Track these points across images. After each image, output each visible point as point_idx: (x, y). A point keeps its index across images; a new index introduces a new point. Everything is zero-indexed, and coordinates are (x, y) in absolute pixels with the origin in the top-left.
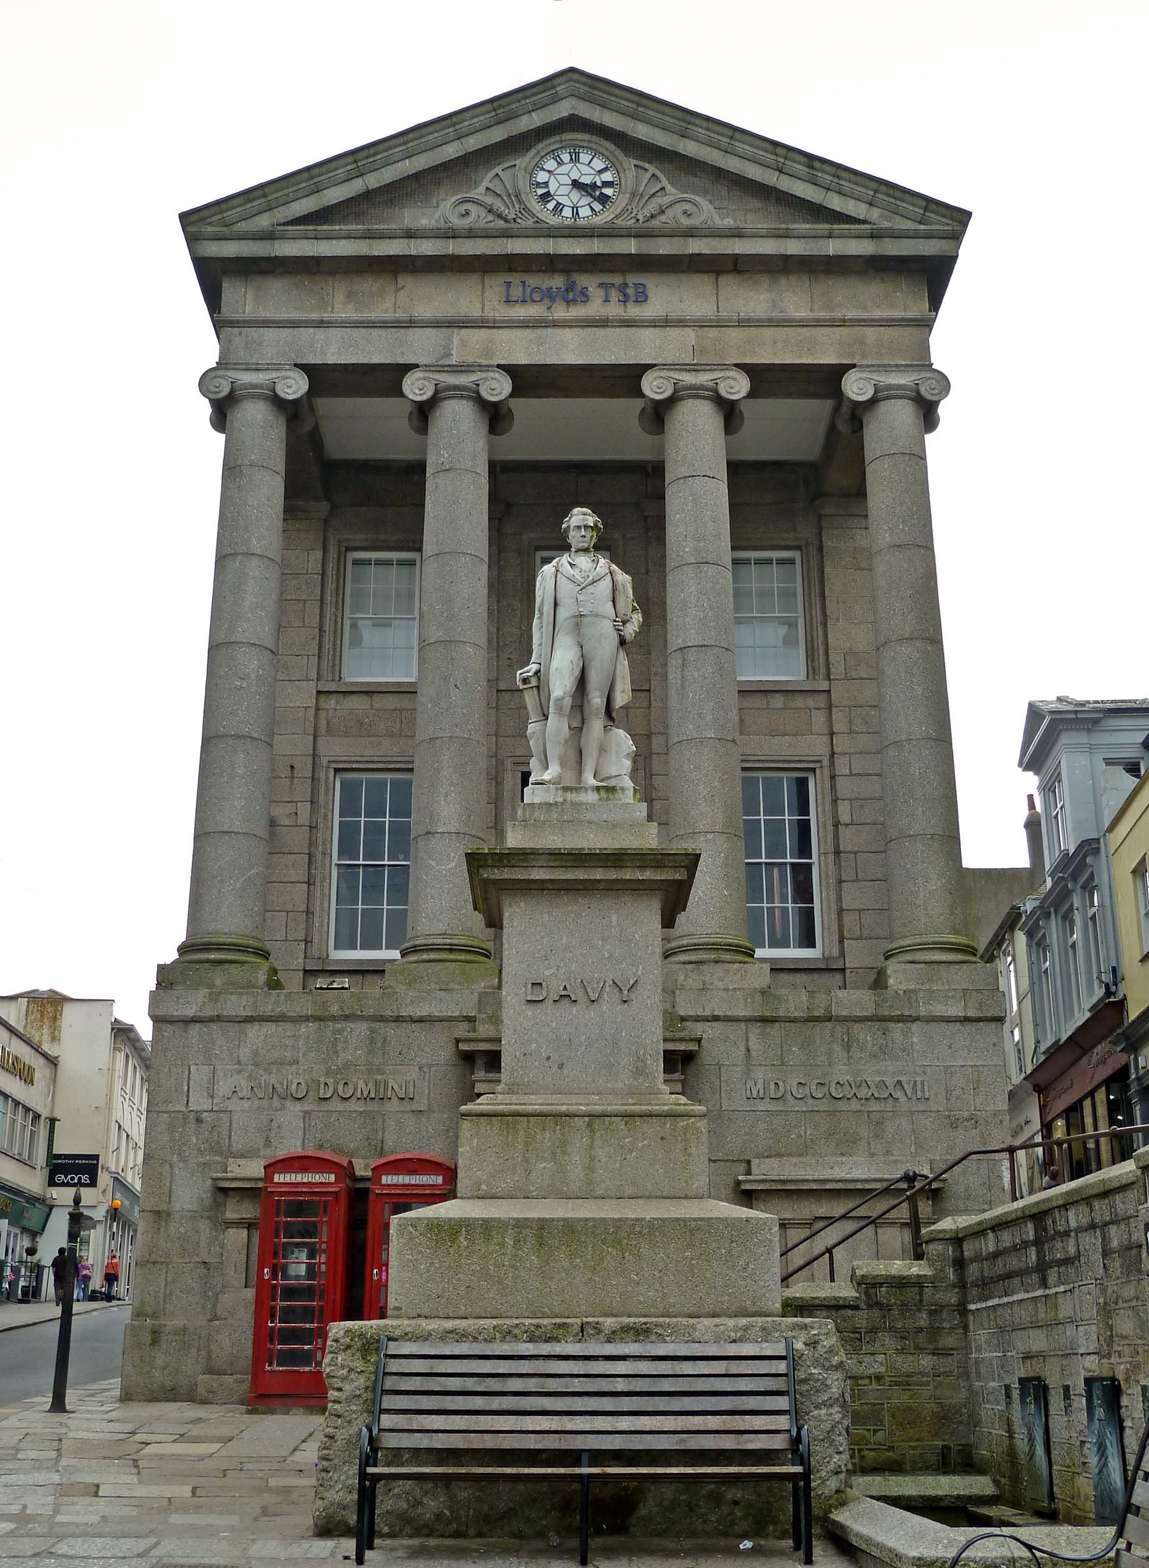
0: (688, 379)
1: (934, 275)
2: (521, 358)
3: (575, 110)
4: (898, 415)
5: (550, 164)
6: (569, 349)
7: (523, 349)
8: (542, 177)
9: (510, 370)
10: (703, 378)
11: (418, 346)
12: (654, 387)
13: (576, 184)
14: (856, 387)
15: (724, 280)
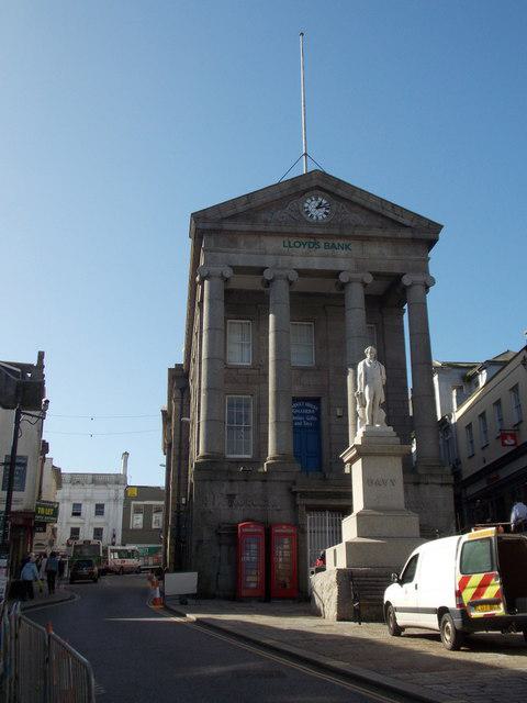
0: (354, 276)
1: (431, 243)
2: (300, 266)
3: (319, 184)
4: (421, 289)
5: (309, 201)
6: (316, 262)
7: (300, 262)
8: (306, 205)
9: (297, 270)
10: (359, 275)
11: (268, 261)
12: (343, 278)
13: (317, 208)
14: (406, 281)
15: (365, 243)
